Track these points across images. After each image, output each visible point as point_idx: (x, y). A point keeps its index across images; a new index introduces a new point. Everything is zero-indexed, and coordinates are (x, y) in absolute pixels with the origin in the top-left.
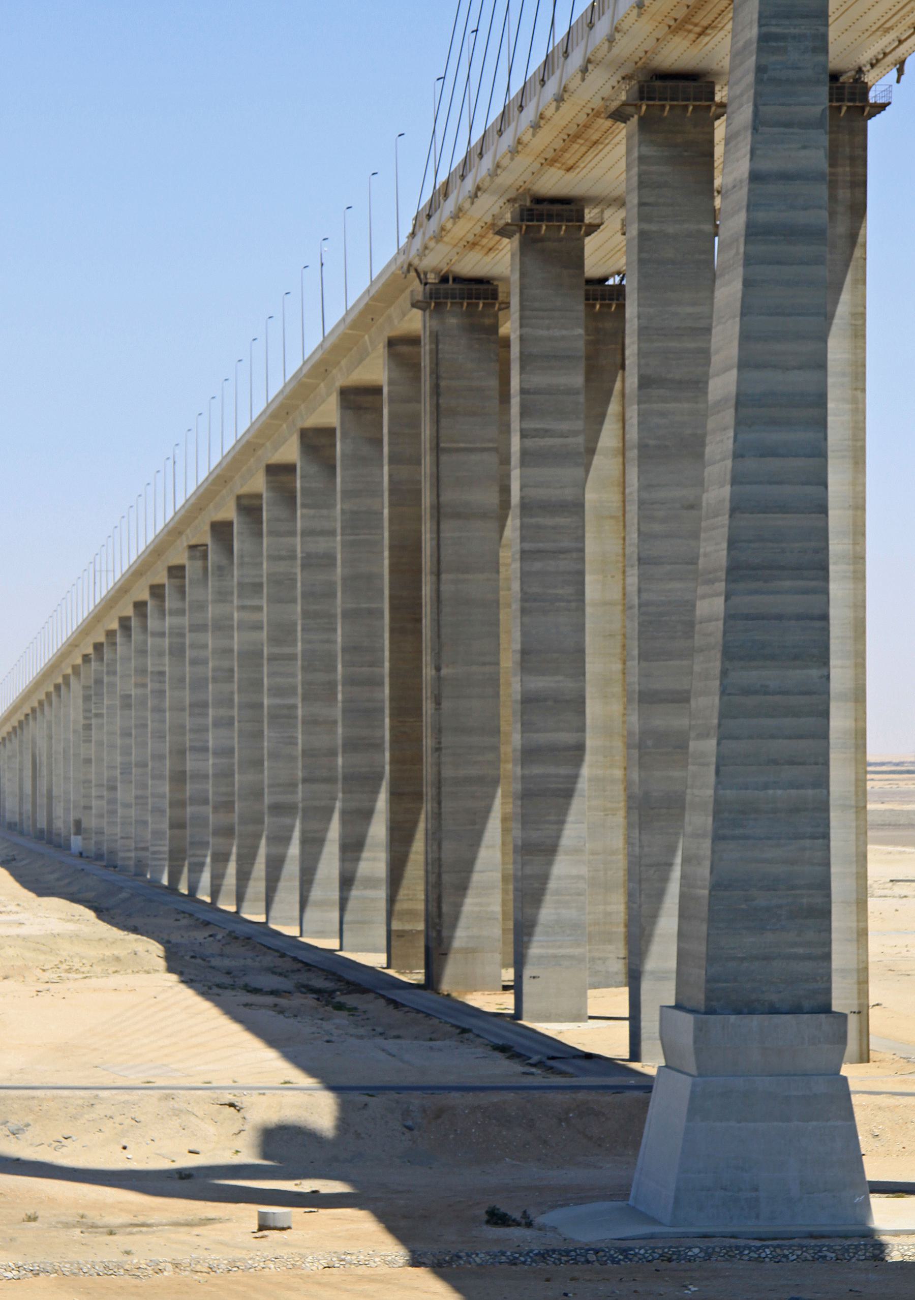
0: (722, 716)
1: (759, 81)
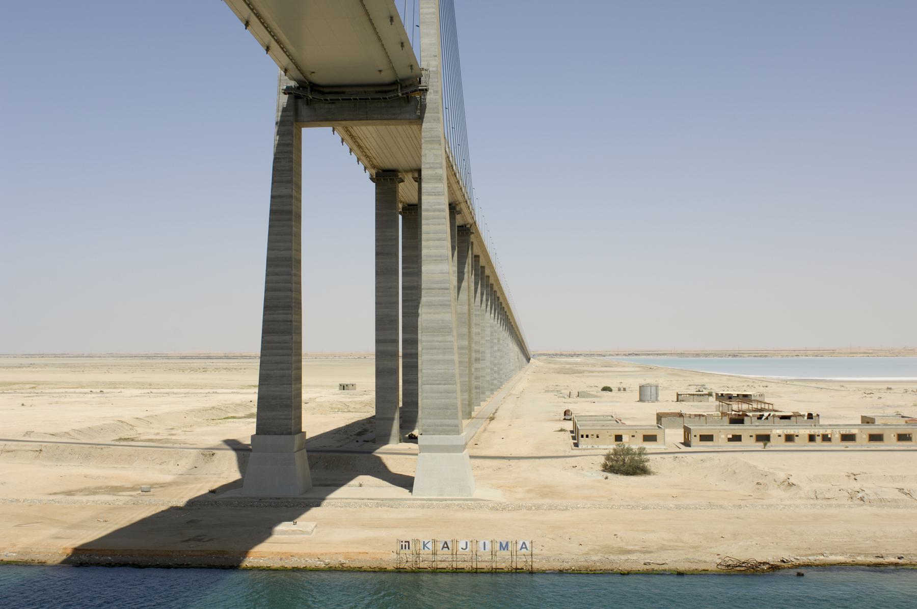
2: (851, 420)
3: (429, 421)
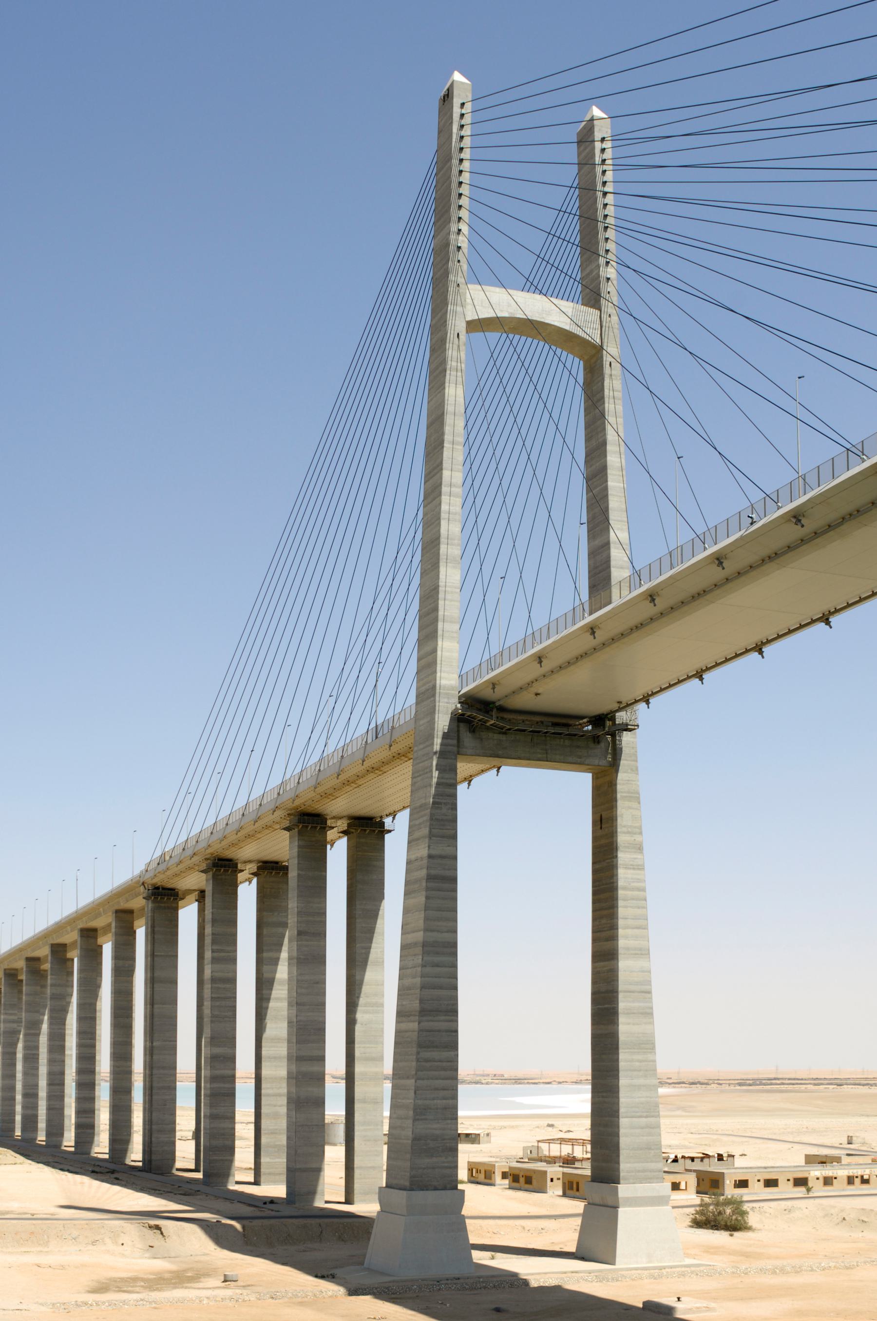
0: (417, 1070)
1: (431, 819)
2: (791, 1159)
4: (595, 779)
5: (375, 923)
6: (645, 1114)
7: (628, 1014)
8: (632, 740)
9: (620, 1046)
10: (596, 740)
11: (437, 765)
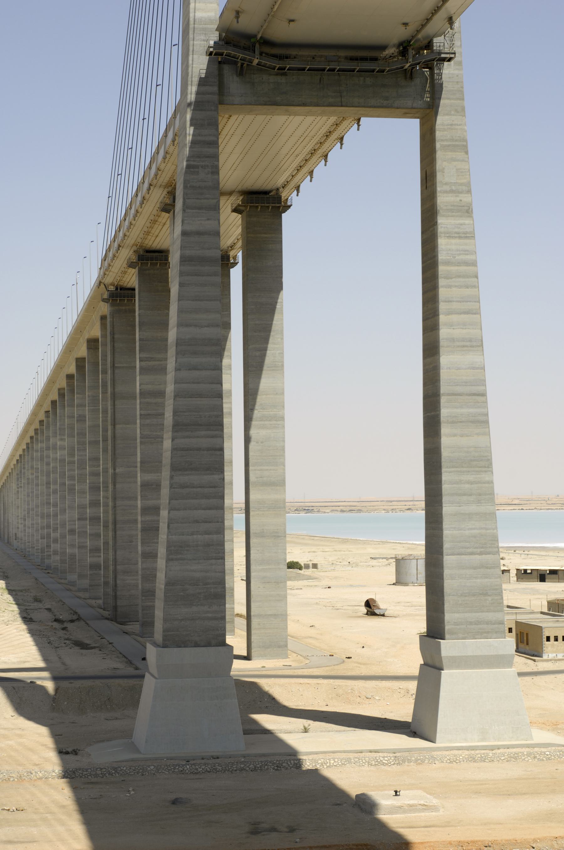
3: (457, 615)
4: (422, 125)
5: (272, 320)
6: (479, 550)
7: (453, 422)
8: (456, 72)
9: (443, 464)
10: (409, 75)
11: (192, 120)
